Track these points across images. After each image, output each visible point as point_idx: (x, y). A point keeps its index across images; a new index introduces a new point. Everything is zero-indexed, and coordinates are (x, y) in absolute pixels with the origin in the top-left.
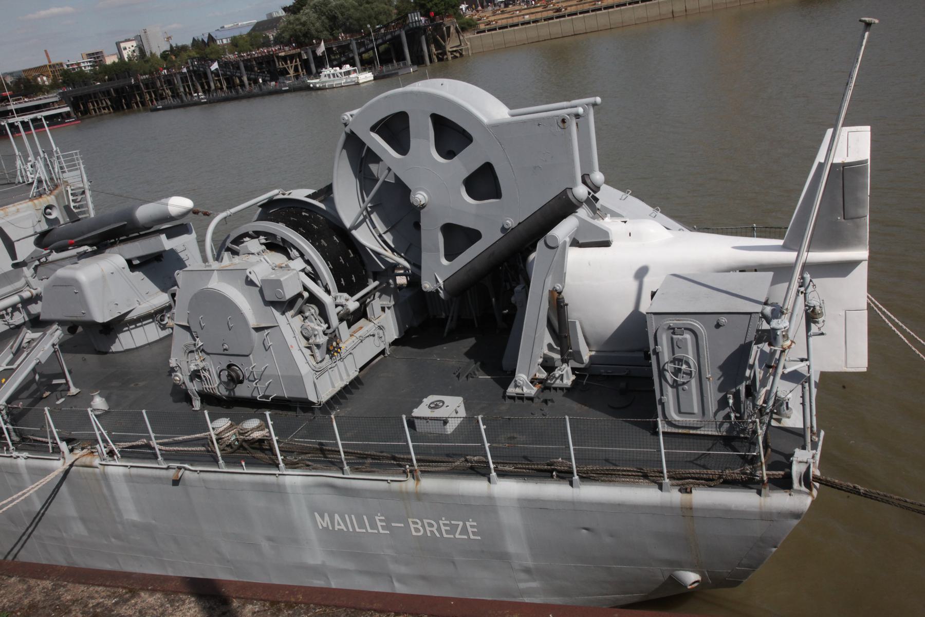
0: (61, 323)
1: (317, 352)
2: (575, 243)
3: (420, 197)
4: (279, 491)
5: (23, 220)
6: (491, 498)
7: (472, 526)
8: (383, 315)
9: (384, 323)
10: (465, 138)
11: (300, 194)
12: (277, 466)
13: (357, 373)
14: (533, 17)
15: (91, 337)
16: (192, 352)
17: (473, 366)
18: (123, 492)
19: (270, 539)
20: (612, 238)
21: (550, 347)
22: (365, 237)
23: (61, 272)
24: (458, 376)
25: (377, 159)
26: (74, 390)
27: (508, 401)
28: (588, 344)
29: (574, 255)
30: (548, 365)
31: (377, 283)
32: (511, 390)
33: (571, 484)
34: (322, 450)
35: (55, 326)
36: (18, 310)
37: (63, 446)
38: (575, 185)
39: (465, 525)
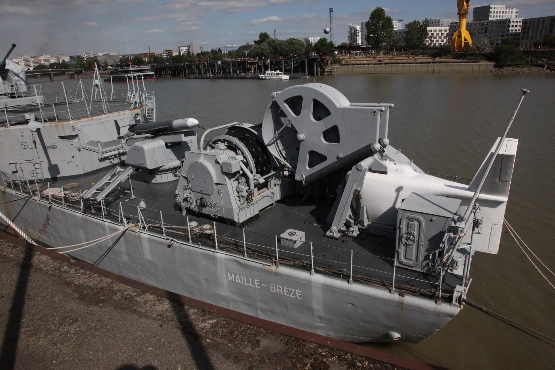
0: (133, 166)
1: (242, 199)
2: (370, 170)
3: (301, 136)
4: (214, 259)
5: (126, 118)
6: (309, 281)
7: (298, 293)
8: (275, 188)
9: (274, 192)
10: (327, 112)
11: (247, 126)
12: (215, 248)
13: (258, 212)
14: (368, 62)
15: (144, 174)
16: (186, 189)
17: (312, 219)
18: (146, 246)
19: (206, 280)
20: (388, 170)
21: (350, 216)
22: (273, 150)
23: (137, 144)
24: (305, 222)
25: (284, 115)
26: (133, 197)
27: (326, 238)
28: (368, 218)
29: (369, 176)
30: (348, 225)
31: (275, 172)
32: (328, 233)
33: (348, 282)
34: (236, 244)
35: (130, 167)
36: (117, 157)
37: (125, 220)
38: (375, 143)
39: (295, 292)
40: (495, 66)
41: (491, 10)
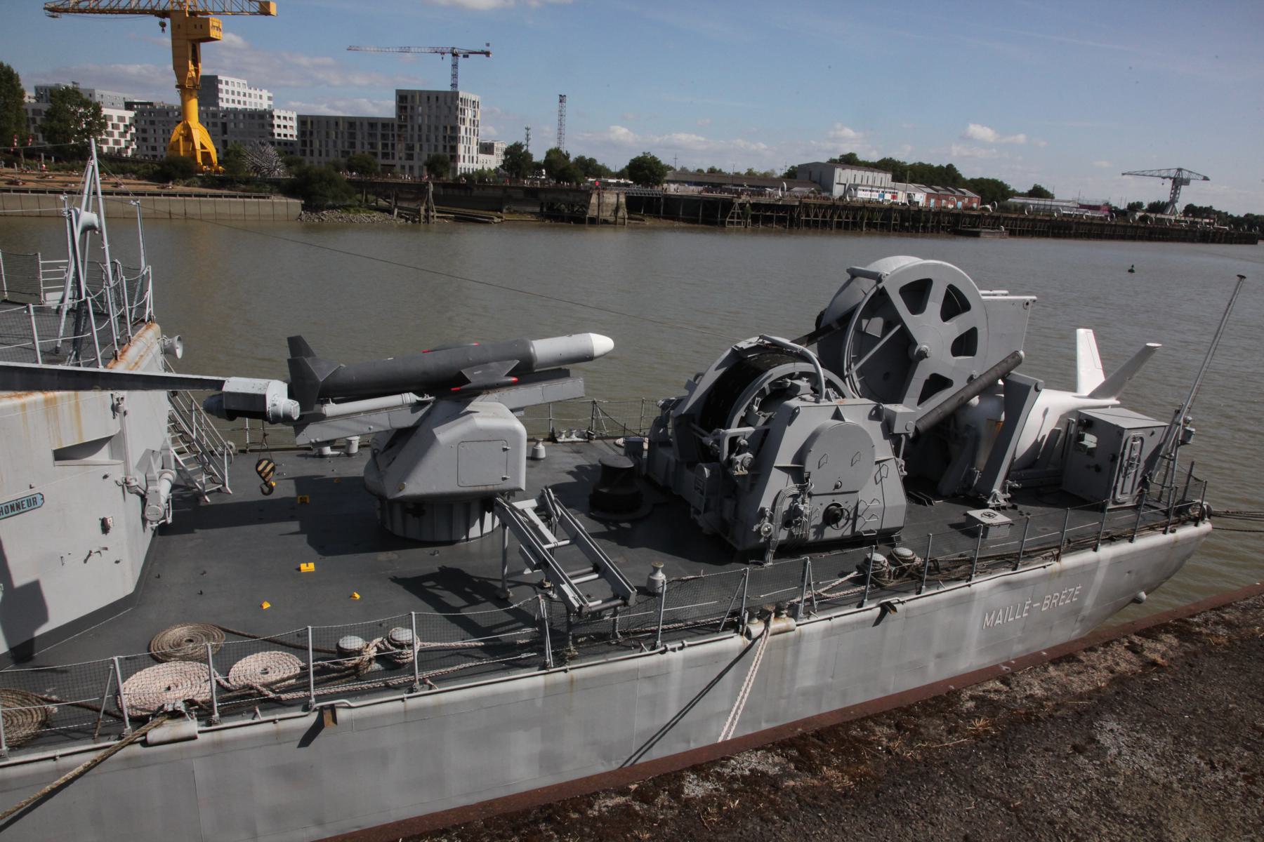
40: (304, 208)
41: (220, 86)
